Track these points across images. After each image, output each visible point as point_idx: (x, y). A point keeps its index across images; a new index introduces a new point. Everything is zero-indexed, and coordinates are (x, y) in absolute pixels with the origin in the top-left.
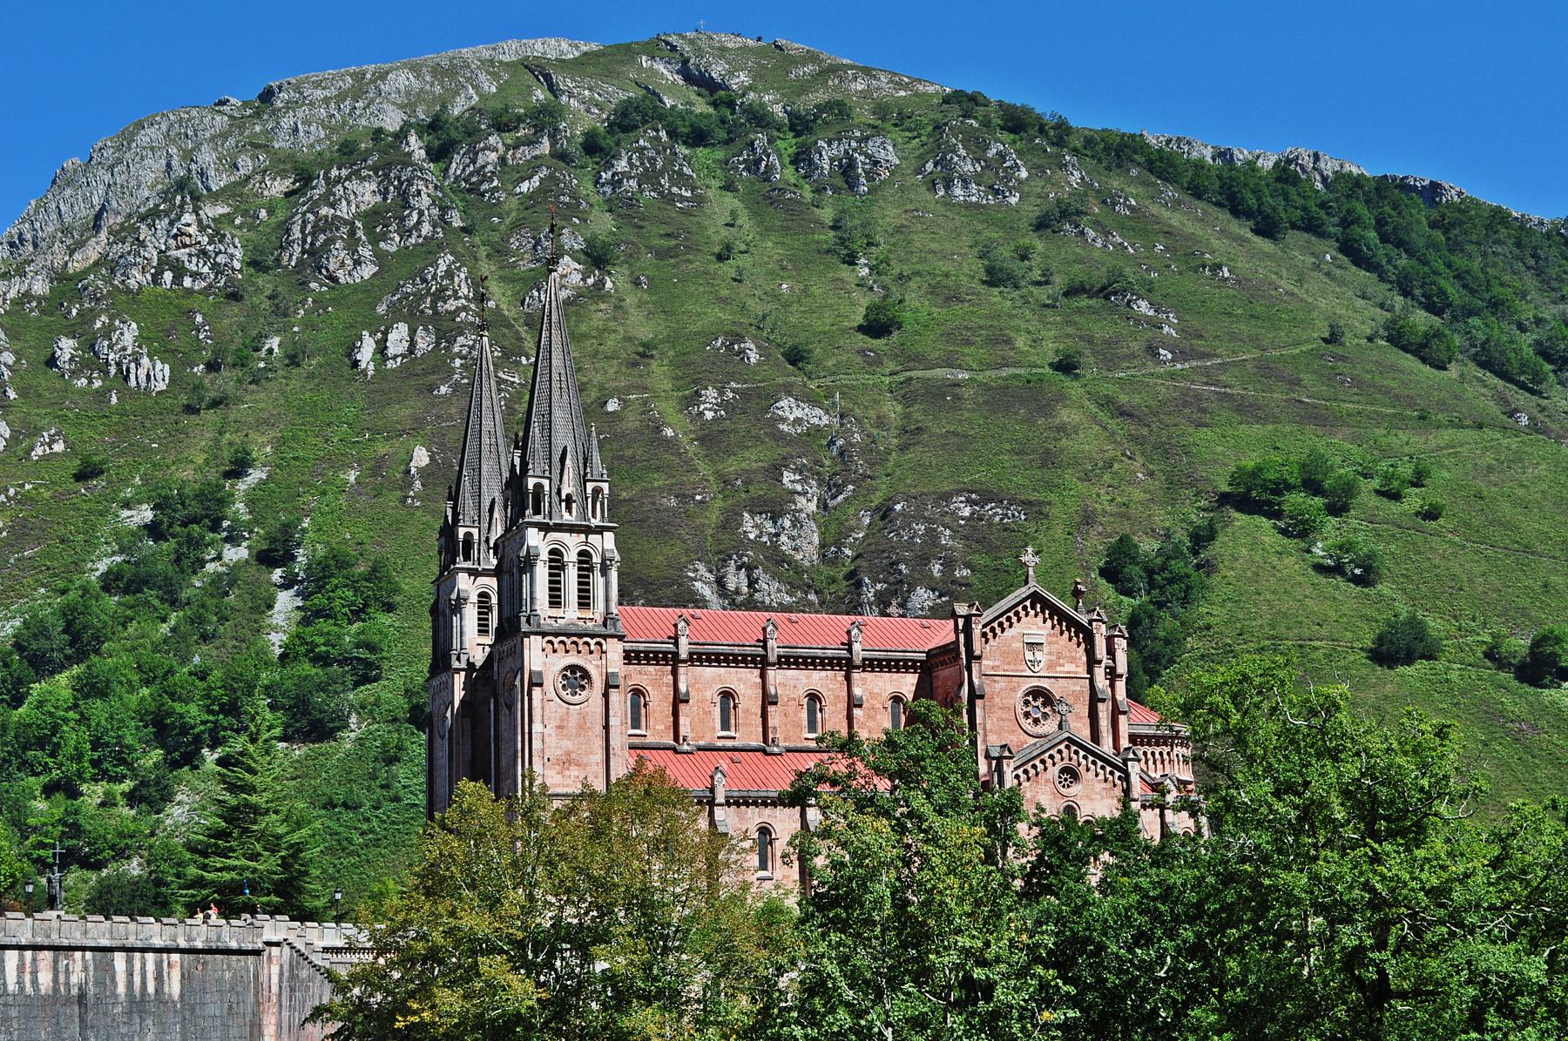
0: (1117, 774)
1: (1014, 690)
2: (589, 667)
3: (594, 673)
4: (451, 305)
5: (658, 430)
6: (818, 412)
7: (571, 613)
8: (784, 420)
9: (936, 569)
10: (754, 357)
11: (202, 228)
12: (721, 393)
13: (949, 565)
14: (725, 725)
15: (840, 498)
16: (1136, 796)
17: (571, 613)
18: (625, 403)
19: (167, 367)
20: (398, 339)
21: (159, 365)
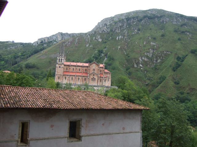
4: (125, 34)
5: (140, 45)
9: (161, 58)
10: (150, 39)
11: (106, 28)
13: (163, 57)
14: (73, 70)
17: (60, 63)
20: (120, 37)
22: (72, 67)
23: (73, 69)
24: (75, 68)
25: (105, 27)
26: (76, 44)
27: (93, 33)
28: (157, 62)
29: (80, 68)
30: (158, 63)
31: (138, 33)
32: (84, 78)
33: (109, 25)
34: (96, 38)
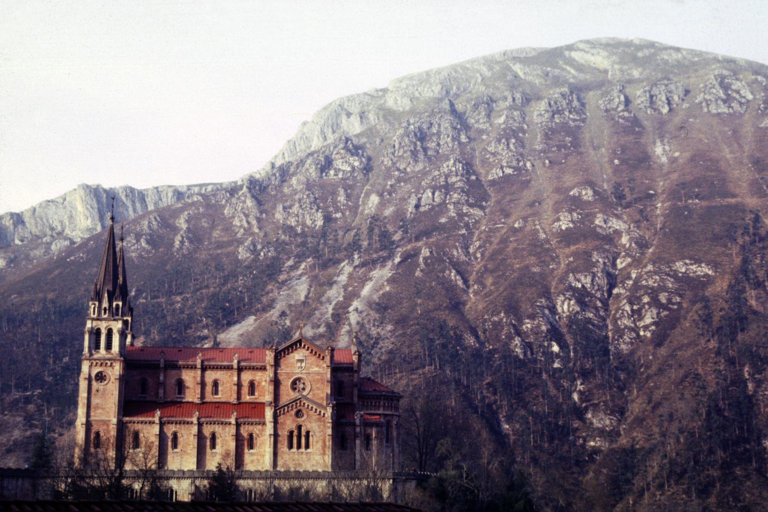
4: (454, 179)
6: (621, 223)
26: (182, 242)
28: (642, 324)
30: (646, 328)
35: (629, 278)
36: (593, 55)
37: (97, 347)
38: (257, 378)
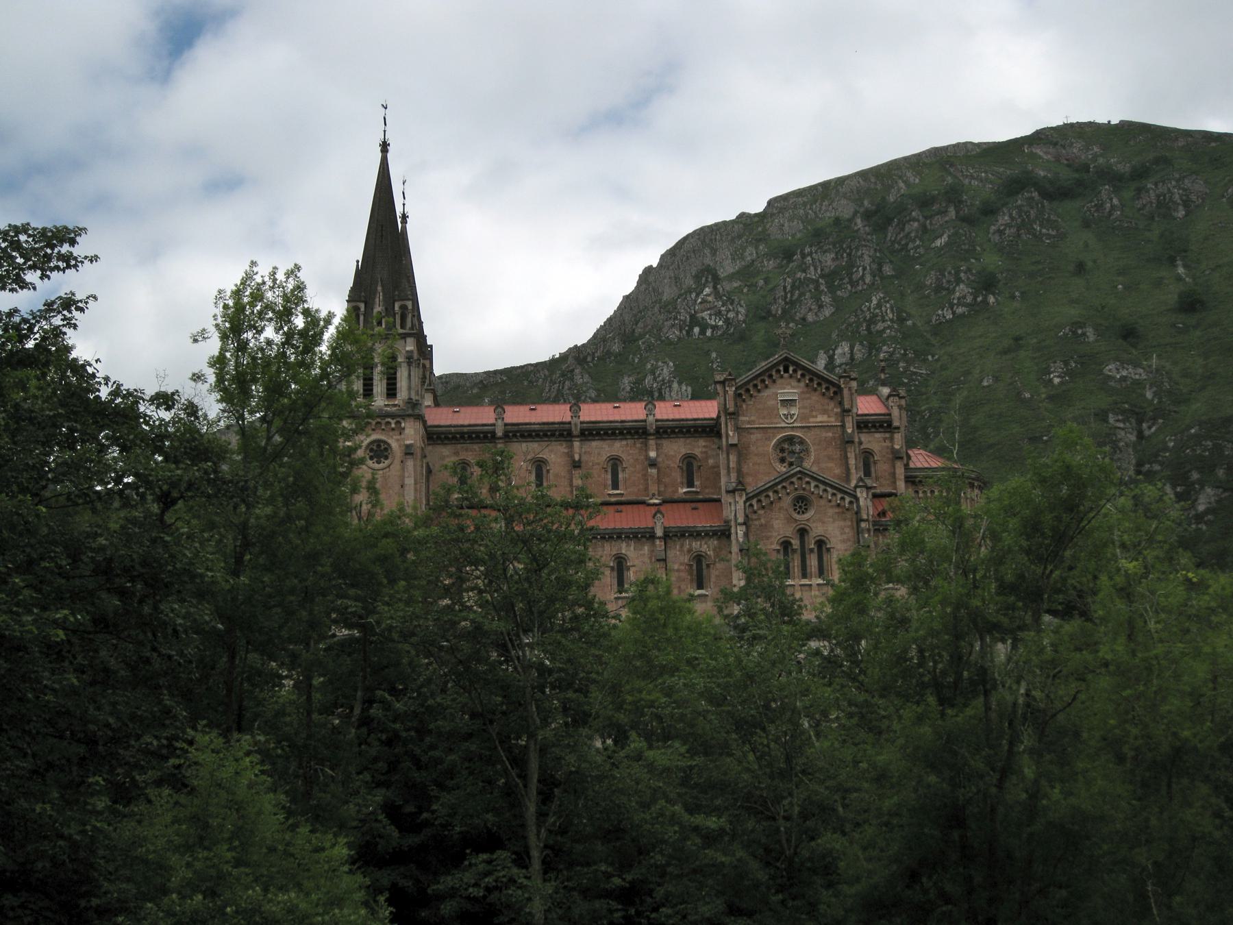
0: (848, 499)
1: (769, 439)
2: (390, 441)
3: (394, 445)
4: (880, 326)
5: (1019, 394)
7: (380, 401)
8: (1113, 378)
12: (1066, 363)
15: (1153, 429)
16: (865, 517)
18: (996, 379)
19: (689, 389)
21: (684, 388)
22: (523, 451)
23: (540, 466)
24: (554, 454)
25: (707, 291)
27: (616, 348)
29: (617, 447)
30: (1199, 518)
31: (978, 308)
32: (679, 556)
33: (731, 277)
34: (639, 381)
35: (1166, 449)
36: (1063, 147)
37: (368, 391)
38: (697, 452)
